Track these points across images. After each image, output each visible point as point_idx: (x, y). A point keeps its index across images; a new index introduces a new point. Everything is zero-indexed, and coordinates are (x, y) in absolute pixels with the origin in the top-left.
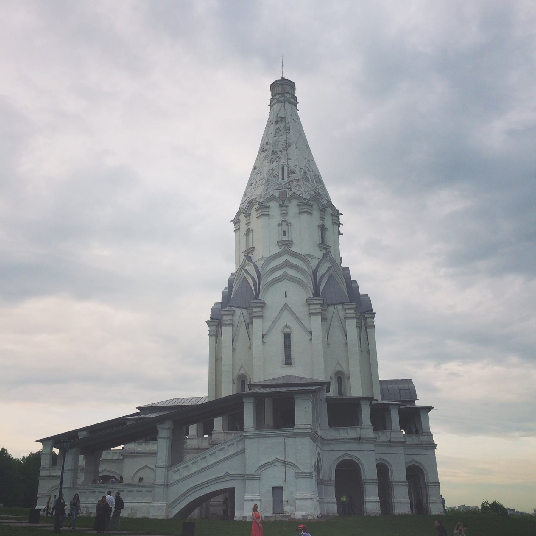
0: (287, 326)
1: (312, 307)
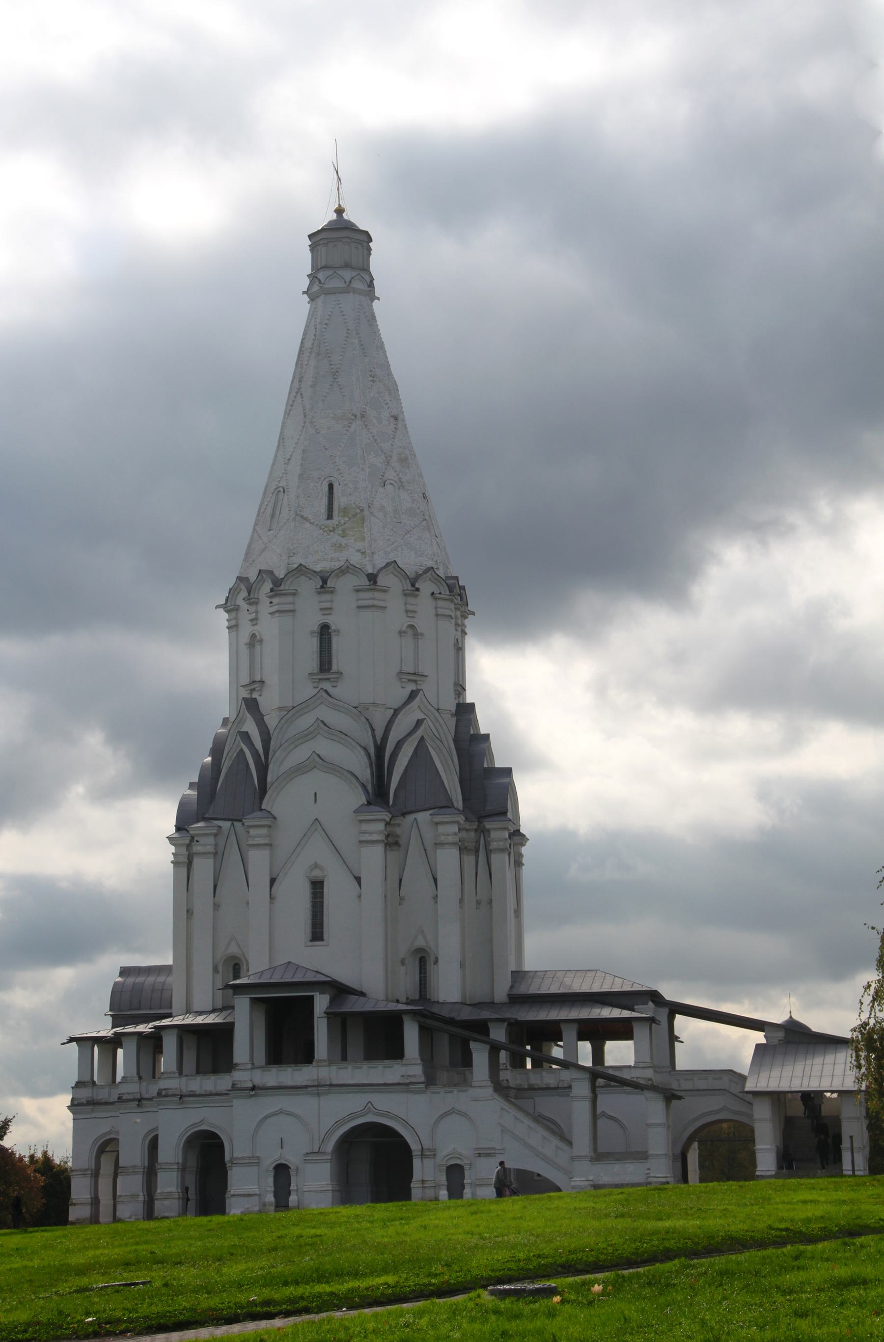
0: (316, 866)
1: (365, 827)
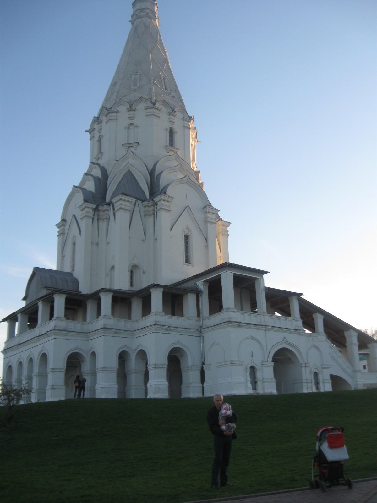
1: (209, 215)
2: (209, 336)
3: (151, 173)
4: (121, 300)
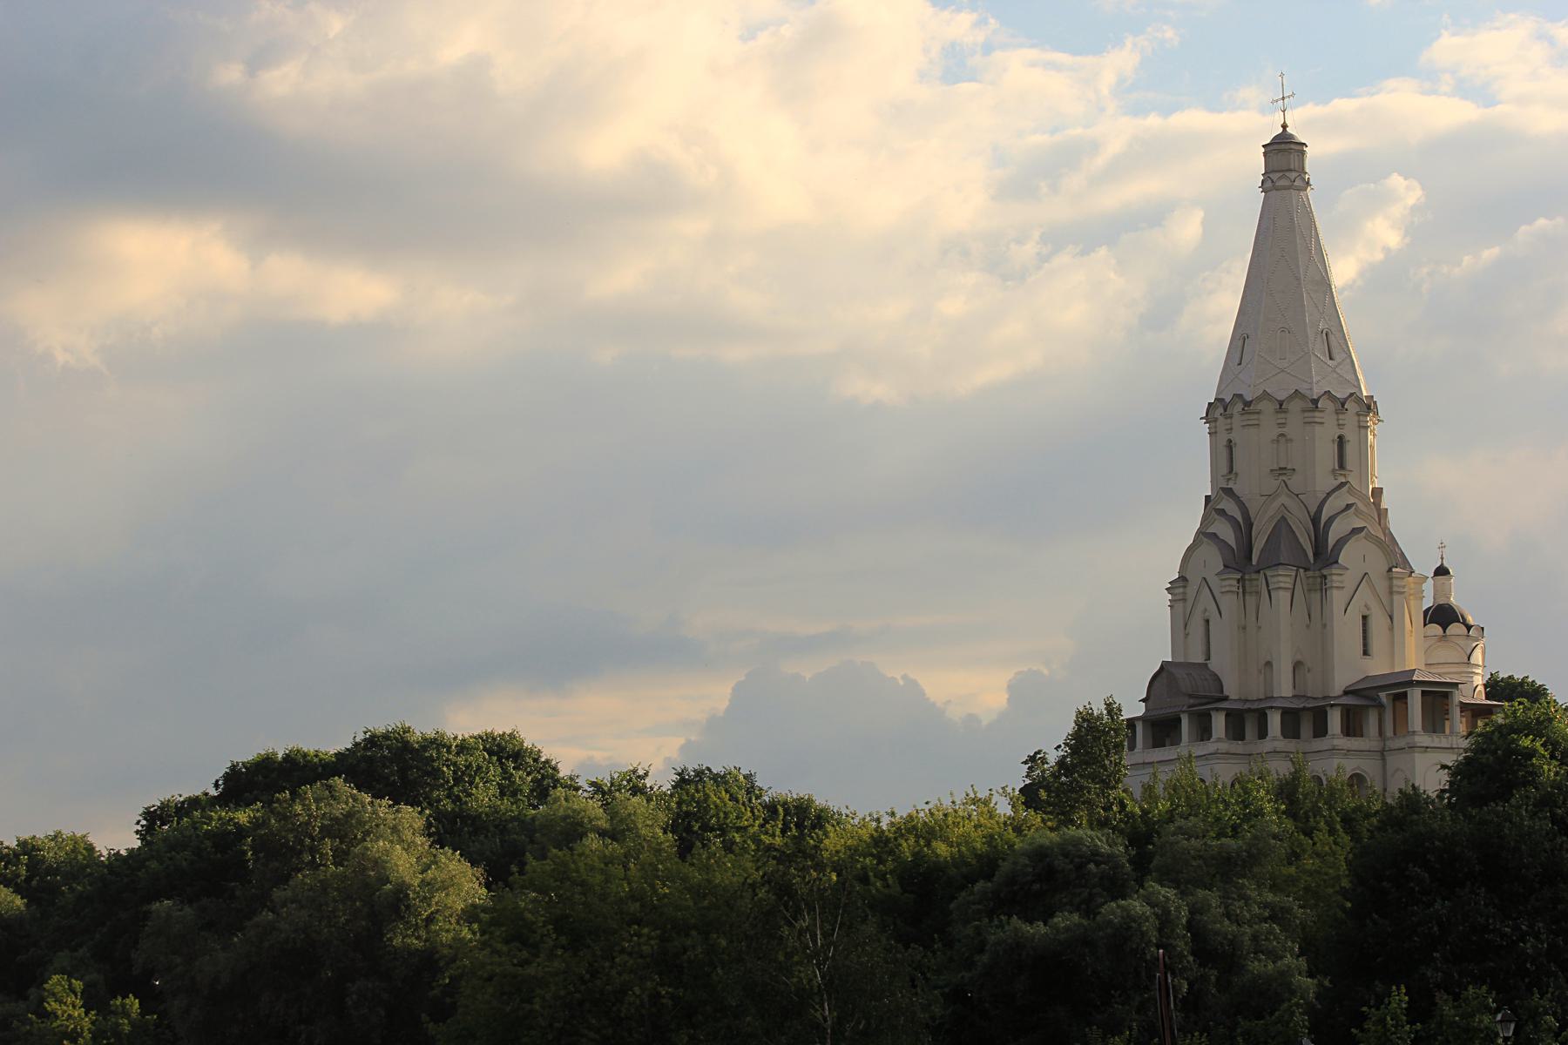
2: (1392, 760)
3: (1315, 520)
4: (1292, 721)
